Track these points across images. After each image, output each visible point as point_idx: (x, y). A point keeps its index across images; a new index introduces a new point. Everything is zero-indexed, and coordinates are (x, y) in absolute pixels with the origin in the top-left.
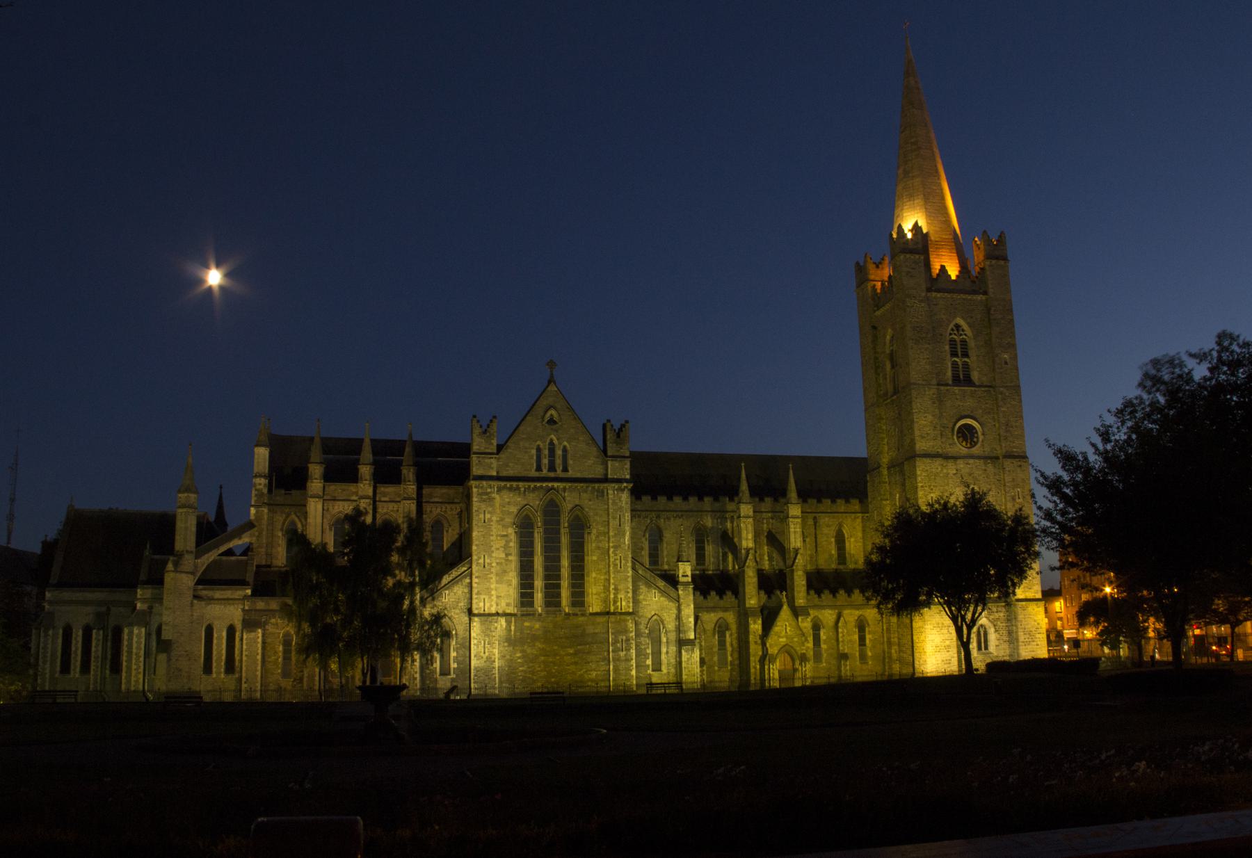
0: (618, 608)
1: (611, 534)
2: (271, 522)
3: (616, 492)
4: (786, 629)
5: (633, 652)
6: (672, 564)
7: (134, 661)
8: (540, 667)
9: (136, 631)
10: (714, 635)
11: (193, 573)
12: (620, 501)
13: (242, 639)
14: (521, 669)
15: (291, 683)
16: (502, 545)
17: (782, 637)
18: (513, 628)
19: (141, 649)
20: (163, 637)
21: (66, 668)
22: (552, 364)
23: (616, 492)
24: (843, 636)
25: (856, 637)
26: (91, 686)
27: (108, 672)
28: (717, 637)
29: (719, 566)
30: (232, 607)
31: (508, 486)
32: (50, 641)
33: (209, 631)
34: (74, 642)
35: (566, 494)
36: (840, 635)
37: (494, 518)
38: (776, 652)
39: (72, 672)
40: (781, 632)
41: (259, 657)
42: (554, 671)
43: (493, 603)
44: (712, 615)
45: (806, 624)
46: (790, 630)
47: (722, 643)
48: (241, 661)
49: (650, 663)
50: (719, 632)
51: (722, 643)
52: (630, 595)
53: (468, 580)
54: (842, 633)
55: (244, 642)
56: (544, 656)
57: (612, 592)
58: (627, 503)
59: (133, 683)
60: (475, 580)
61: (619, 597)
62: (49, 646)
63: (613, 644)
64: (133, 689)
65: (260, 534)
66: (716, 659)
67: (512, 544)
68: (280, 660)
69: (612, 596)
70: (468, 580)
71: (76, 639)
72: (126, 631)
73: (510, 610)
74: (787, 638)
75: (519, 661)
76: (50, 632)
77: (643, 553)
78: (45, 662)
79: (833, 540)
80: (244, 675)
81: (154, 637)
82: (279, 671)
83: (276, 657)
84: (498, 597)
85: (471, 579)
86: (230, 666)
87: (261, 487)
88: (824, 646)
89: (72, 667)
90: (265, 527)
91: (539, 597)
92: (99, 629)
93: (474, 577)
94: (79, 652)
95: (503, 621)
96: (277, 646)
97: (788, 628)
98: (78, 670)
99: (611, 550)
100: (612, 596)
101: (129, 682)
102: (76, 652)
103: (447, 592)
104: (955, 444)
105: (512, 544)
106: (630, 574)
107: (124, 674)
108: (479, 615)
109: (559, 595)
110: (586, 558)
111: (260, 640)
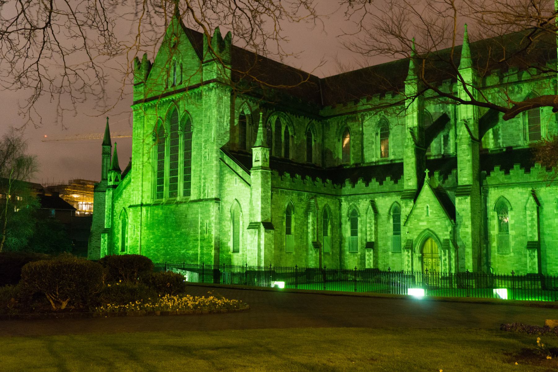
0: (205, 195)
1: (204, 130)
4: (428, 211)
6: (397, 154)
8: (162, 246)
10: (389, 219)
14: (152, 247)
17: (423, 221)
18: (149, 215)
24: (533, 220)
28: (391, 220)
29: (441, 151)
31: (150, 105)
36: (529, 218)
38: (415, 237)
40: (421, 216)
42: (169, 250)
44: (387, 199)
46: (432, 213)
50: (394, 217)
54: (531, 216)
56: (164, 237)
61: (207, 185)
63: (201, 227)
66: (390, 243)
73: (149, 201)
74: (428, 222)
75: (151, 241)
77: (374, 146)
88: (512, 232)
91: (166, 190)
97: (430, 211)
99: (203, 144)
100: (202, 185)
103: (125, 190)
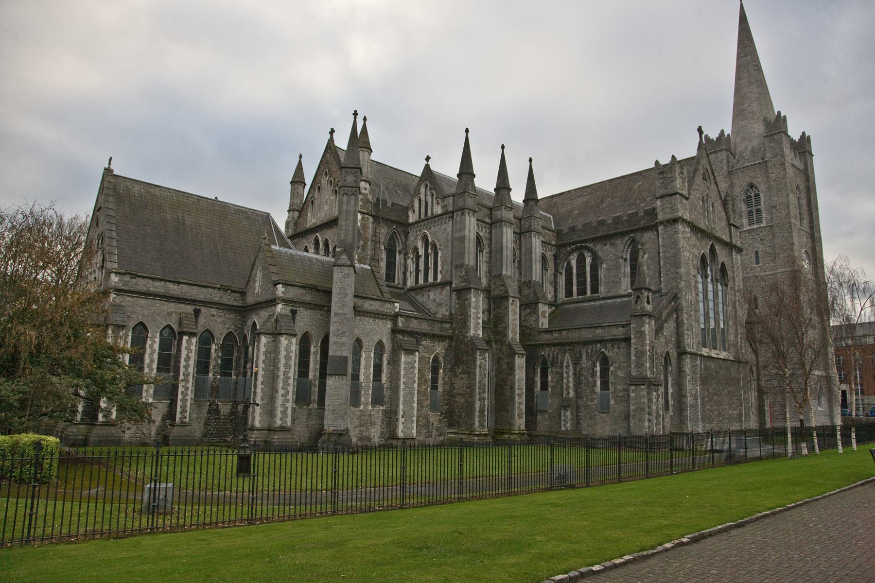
2: (374, 235)
7: (281, 384)
13: (394, 362)
15: (438, 417)
19: (290, 366)
20: (331, 353)
30: (380, 322)
41: (416, 385)
64: (279, 423)
65: (365, 243)
68: (429, 389)
71: (151, 346)
82: (428, 403)
83: (426, 387)
87: (367, 192)
90: (370, 237)
92: (192, 335)
94: (155, 366)
96: (426, 374)
101: (270, 412)
102: (150, 366)
103: (666, 325)
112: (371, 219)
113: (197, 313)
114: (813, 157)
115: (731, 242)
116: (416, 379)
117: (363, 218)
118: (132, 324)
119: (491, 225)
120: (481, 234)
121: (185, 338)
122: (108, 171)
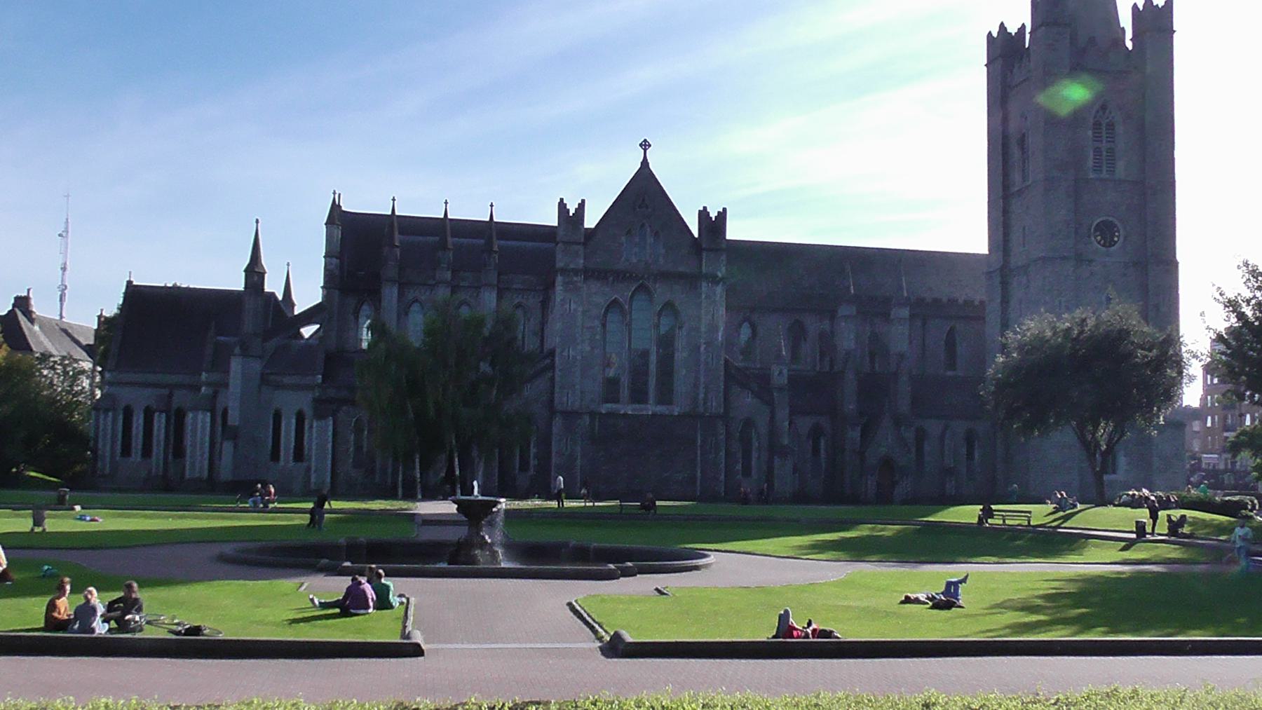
3: (710, 285)
5: (722, 454)
9: (200, 416)
11: (260, 357)
12: (715, 294)
13: (311, 427)
16: (588, 337)
18: (597, 424)
20: (229, 423)
21: (126, 450)
22: (645, 145)
23: (710, 285)
25: (964, 451)
26: (154, 471)
27: (170, 457)
32: (109, 423)
33: (277, 417)
34: (135, 426)
35: (657, 286)
37: (580, 309)
39: (133, 455)
41: (330, 446)
43: (576, 398)
45: (909, 435)
47: (816, 451)
48: (310, 450)
49: (740, 468)
51: (816, 451)
52: (721, 395)
53: (550, 374)
55: (314, 430)
57: (702, 390)
58: (721, 297)
59: (197, 470)
60: (558, 373)
61: (710, 397)
62: (110, 428)
63: (701, 446)
64: (197, 475)
67: (598, 337)
69: (702, 396)
70: (550, 374)
72: (190, 415)
76: (110, 414)
78: (104, 445)
79: (943, 343)
80: (313, 464)
81: (219, 420)
84: (582, 392)
85: (553, 372)
86: (299, 454)
89: (134, 450)
92: (161, 412)
93: (557, 370)
95: (587, 419)
98: (140, 453)
100: (702, 396)
102: (137, 434)
104: (1091, 243)
105: (598, 337)
106: (722, 373)
107: (188, 458)
108: (562, 412)
109: (646, 393)
110: (676, 355)
111: (331, 428)
112: (337, 292)
113: (170, 396)
114: (1177, 38)
115: (701, 272)
116: (330, 439)
117: (328, 293)
118: (123, 405)
119: (434, 285)
120: (423, 298)
121: (156, 414)
122: (129, 283)
